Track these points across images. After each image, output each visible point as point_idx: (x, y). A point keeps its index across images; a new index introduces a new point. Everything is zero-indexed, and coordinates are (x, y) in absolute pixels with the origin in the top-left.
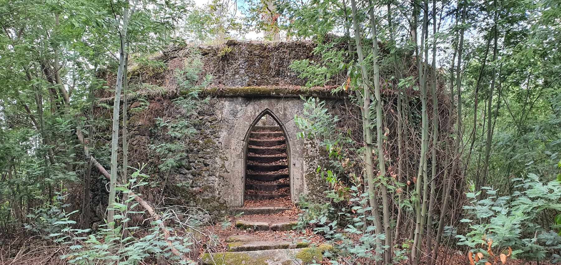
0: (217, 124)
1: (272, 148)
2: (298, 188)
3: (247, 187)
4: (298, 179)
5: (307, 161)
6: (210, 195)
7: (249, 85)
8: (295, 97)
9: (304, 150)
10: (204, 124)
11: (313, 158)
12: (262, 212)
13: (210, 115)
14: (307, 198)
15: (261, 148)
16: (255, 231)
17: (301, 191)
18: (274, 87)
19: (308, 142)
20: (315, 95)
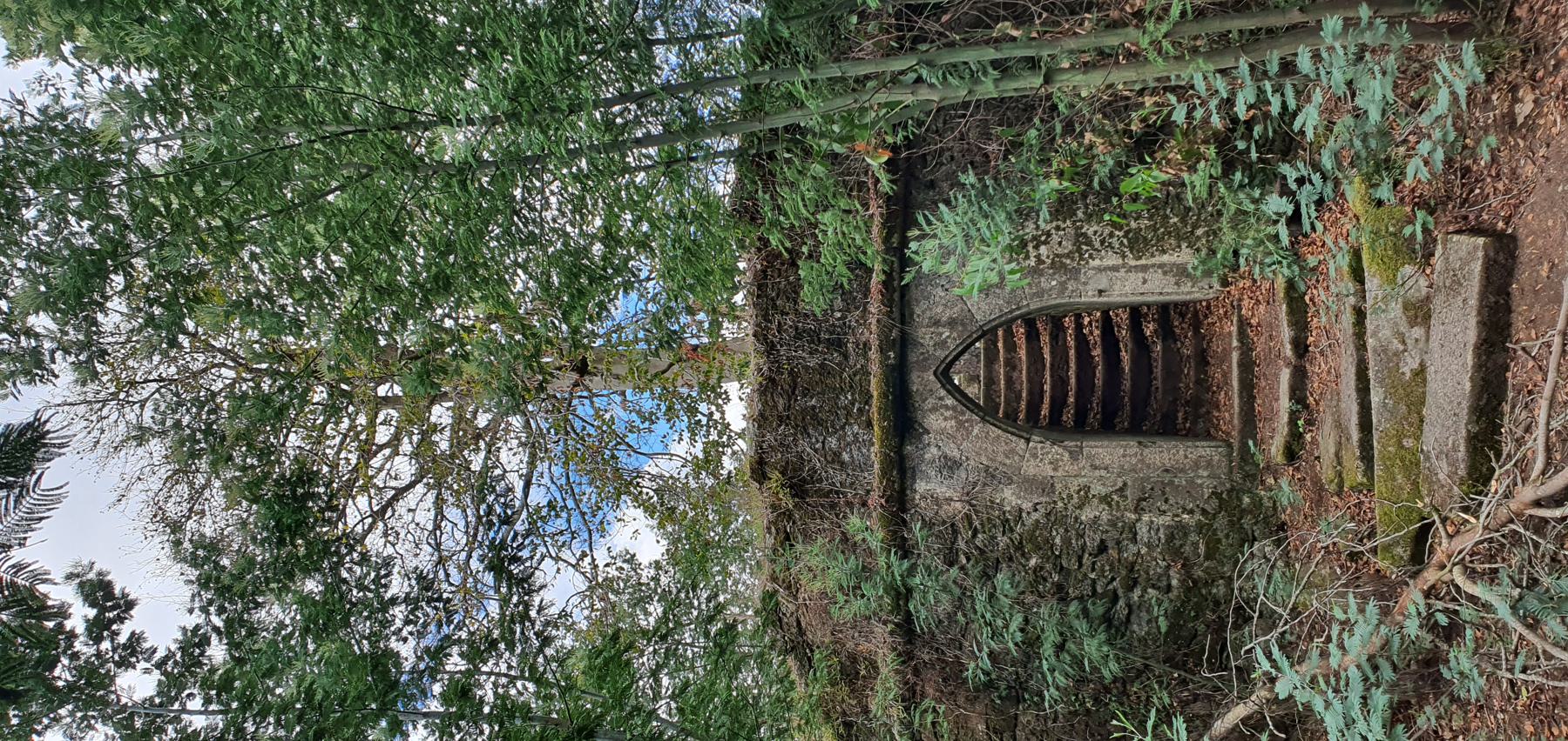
0: (984, 518)
1: (1047, 356)
2: (1173, 280)
3: (1168, 429)
4: (1145, 282)
5: (1091, 256)
6: (1193, 537)
7: (869, 424)
8: (902, 296)
9: (1058, 265)
10: (982, 552)
11: (1081, 239)
12: (1248, 387)
13: (955, 532)
14: (1204, 252)
15: (1047, 387)
16: (1306, 407)
17: (1181, 272)
18: (874, 354)
19: (1033, 253)
20: (895, 240)
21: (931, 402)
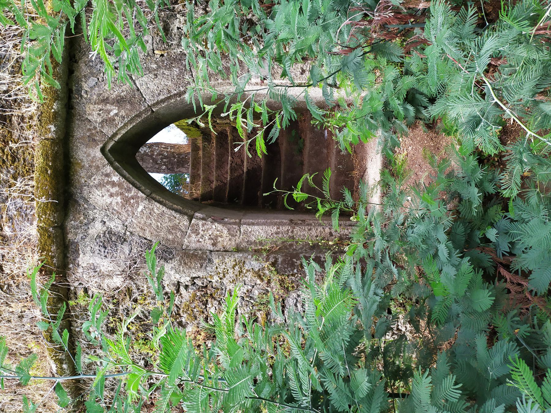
21: (97, 179)
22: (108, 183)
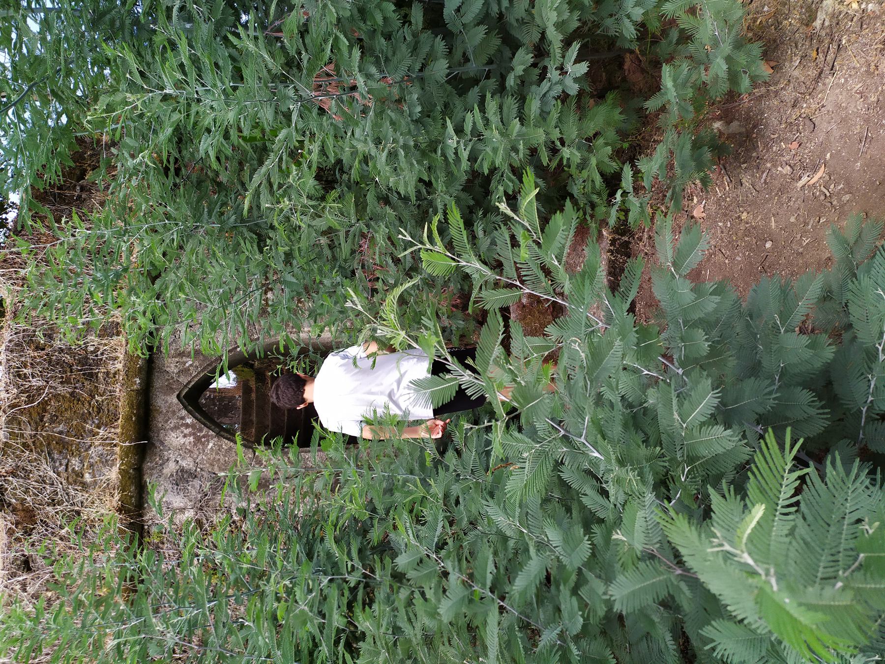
21: (173, 422)
22: (183, 425)
